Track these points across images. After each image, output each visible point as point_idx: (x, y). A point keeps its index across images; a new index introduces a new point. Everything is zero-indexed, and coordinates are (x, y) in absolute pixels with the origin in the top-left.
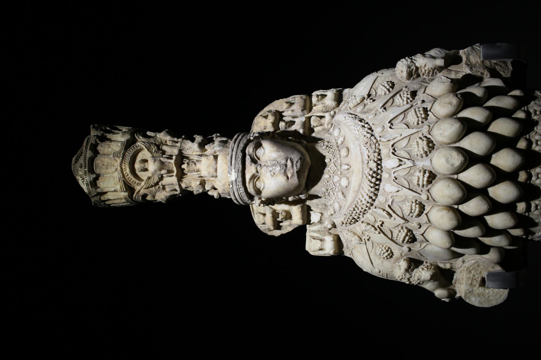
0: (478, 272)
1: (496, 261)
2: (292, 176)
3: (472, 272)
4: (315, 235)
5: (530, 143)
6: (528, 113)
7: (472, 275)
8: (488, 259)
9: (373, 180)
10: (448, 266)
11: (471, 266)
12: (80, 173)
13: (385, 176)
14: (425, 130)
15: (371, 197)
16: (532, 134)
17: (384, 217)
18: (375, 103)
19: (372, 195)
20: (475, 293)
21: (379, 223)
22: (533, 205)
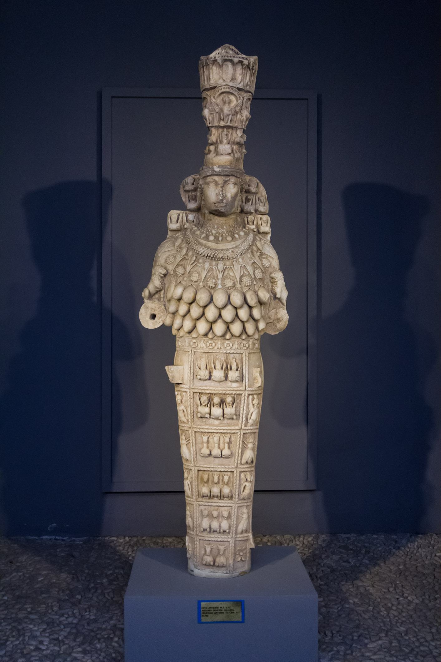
2: (216, 207)
4: (180, 217)
9: (212, 256)
12: (223, 52)
13: (214, 263)
14: (238, 286)
15: (202, 253)
17: (190, 261)
18: (257, 258)
19: (203, 254)
21: (187, 258)
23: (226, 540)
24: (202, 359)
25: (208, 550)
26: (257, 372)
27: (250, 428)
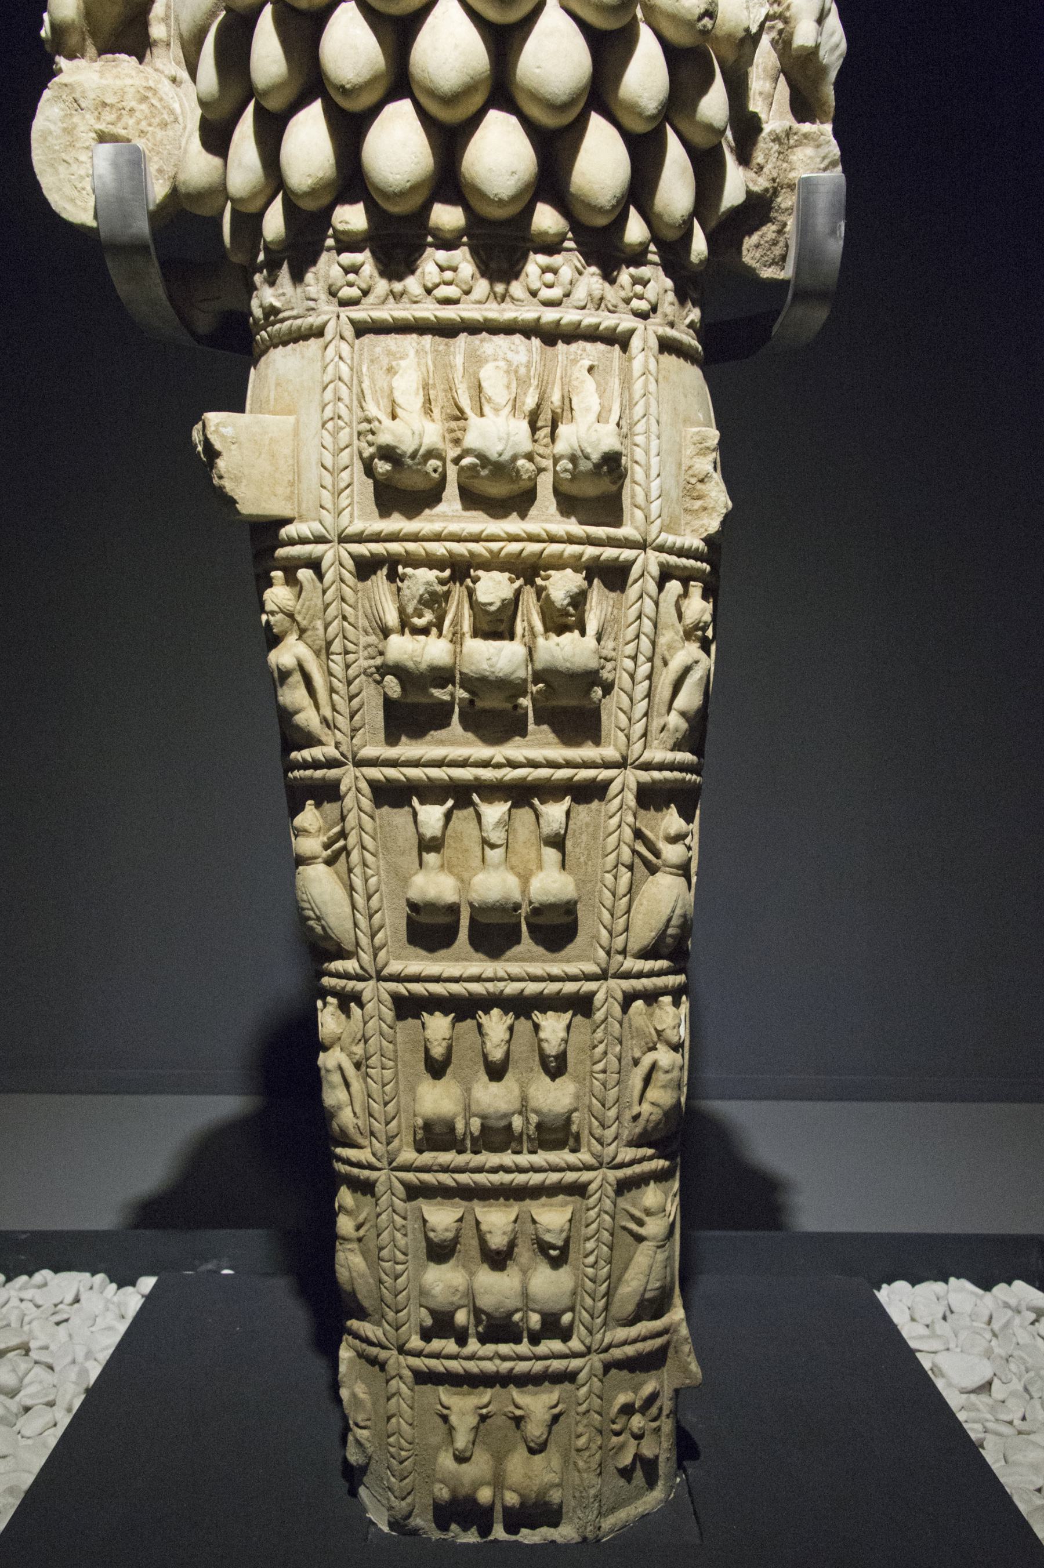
0: (144, 123)
1: (181, 177)
3: (144, 107)
5: (551, 247)
6: (638, 258)
7: (133, 104)
8: (186, 151)
10: (157, 31)
11: (161, 100)
16: (577, 259)
20: (75, 120)
22: (357, 258)
23: (557, 1365)
24: (403, 363)
25: (463, 1423)
26: (703, 452)
27: (670, 756)
